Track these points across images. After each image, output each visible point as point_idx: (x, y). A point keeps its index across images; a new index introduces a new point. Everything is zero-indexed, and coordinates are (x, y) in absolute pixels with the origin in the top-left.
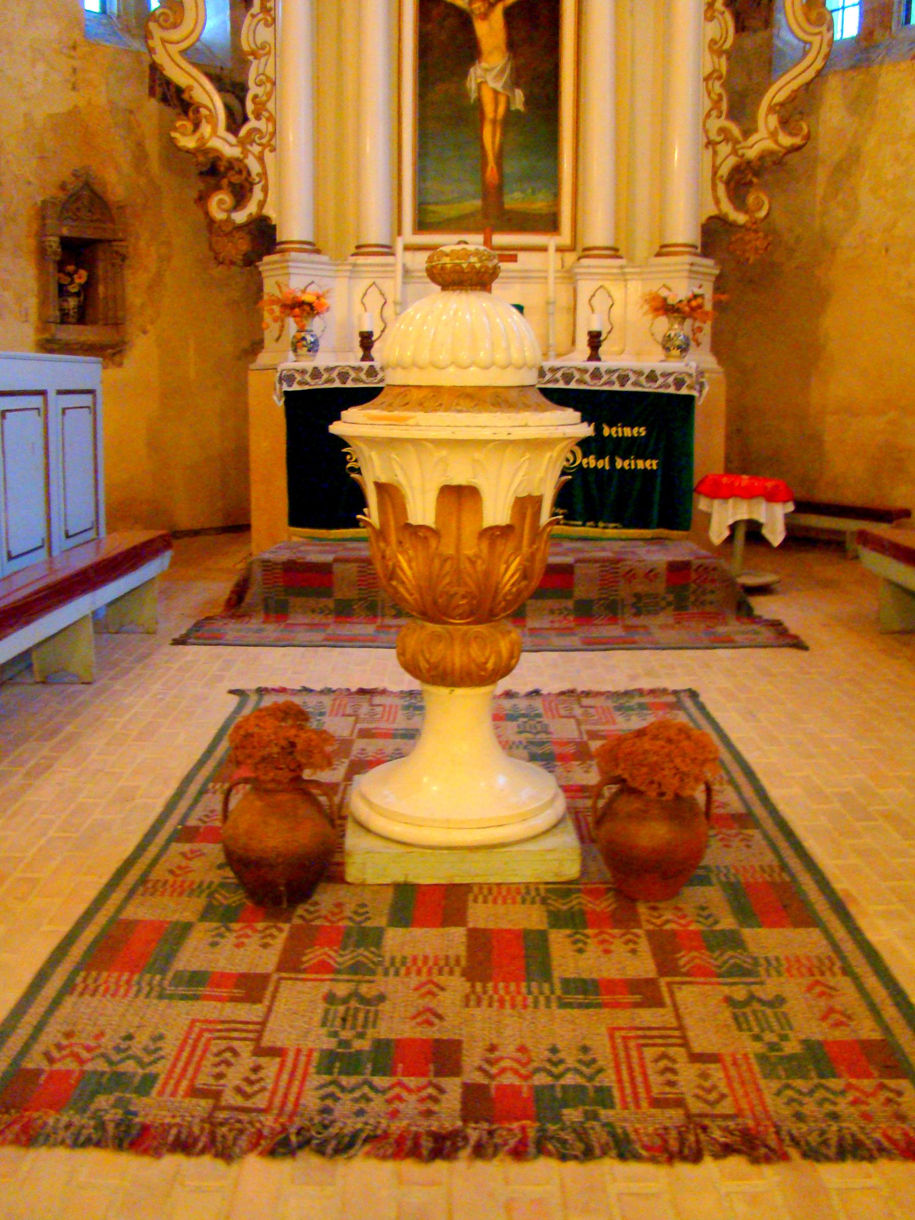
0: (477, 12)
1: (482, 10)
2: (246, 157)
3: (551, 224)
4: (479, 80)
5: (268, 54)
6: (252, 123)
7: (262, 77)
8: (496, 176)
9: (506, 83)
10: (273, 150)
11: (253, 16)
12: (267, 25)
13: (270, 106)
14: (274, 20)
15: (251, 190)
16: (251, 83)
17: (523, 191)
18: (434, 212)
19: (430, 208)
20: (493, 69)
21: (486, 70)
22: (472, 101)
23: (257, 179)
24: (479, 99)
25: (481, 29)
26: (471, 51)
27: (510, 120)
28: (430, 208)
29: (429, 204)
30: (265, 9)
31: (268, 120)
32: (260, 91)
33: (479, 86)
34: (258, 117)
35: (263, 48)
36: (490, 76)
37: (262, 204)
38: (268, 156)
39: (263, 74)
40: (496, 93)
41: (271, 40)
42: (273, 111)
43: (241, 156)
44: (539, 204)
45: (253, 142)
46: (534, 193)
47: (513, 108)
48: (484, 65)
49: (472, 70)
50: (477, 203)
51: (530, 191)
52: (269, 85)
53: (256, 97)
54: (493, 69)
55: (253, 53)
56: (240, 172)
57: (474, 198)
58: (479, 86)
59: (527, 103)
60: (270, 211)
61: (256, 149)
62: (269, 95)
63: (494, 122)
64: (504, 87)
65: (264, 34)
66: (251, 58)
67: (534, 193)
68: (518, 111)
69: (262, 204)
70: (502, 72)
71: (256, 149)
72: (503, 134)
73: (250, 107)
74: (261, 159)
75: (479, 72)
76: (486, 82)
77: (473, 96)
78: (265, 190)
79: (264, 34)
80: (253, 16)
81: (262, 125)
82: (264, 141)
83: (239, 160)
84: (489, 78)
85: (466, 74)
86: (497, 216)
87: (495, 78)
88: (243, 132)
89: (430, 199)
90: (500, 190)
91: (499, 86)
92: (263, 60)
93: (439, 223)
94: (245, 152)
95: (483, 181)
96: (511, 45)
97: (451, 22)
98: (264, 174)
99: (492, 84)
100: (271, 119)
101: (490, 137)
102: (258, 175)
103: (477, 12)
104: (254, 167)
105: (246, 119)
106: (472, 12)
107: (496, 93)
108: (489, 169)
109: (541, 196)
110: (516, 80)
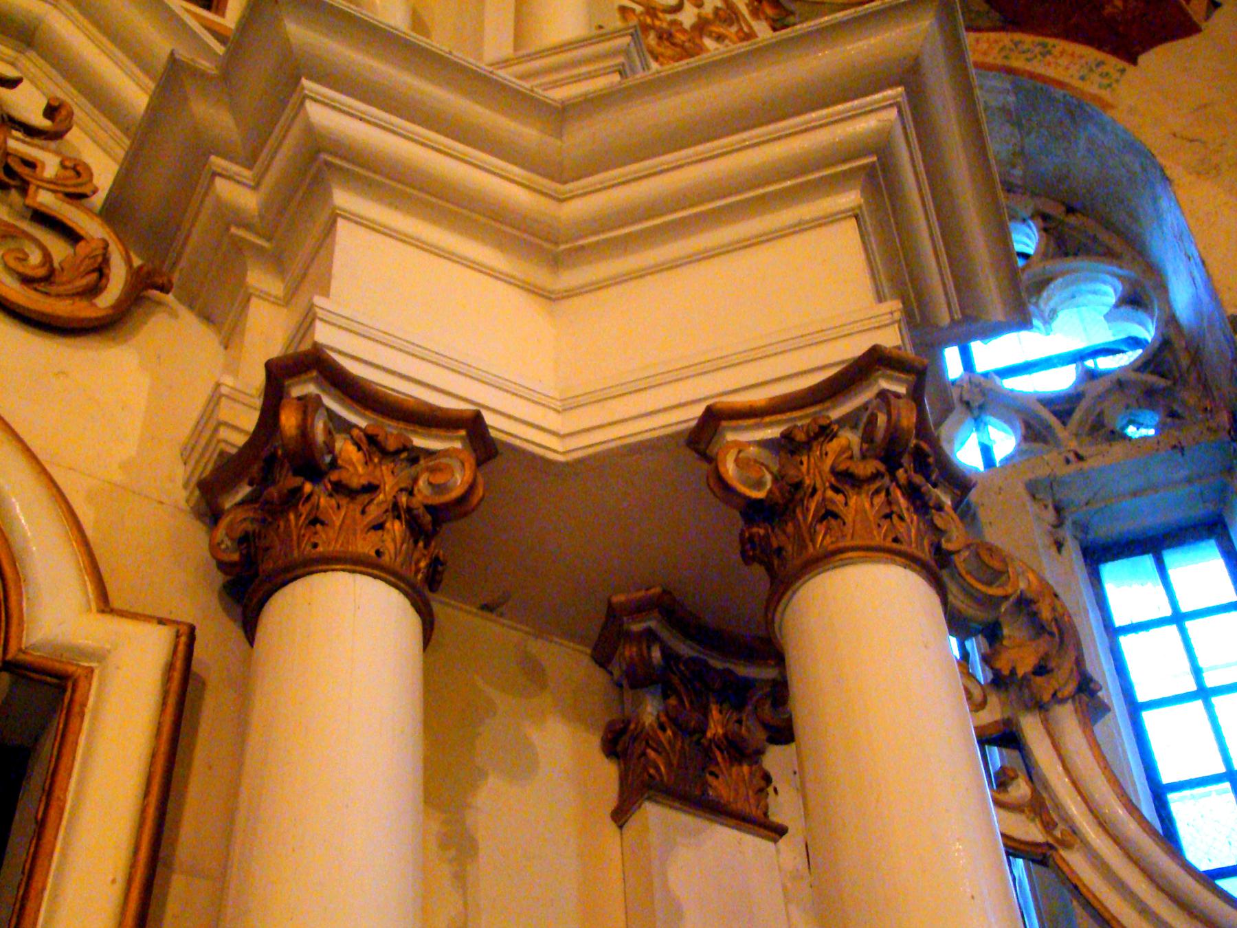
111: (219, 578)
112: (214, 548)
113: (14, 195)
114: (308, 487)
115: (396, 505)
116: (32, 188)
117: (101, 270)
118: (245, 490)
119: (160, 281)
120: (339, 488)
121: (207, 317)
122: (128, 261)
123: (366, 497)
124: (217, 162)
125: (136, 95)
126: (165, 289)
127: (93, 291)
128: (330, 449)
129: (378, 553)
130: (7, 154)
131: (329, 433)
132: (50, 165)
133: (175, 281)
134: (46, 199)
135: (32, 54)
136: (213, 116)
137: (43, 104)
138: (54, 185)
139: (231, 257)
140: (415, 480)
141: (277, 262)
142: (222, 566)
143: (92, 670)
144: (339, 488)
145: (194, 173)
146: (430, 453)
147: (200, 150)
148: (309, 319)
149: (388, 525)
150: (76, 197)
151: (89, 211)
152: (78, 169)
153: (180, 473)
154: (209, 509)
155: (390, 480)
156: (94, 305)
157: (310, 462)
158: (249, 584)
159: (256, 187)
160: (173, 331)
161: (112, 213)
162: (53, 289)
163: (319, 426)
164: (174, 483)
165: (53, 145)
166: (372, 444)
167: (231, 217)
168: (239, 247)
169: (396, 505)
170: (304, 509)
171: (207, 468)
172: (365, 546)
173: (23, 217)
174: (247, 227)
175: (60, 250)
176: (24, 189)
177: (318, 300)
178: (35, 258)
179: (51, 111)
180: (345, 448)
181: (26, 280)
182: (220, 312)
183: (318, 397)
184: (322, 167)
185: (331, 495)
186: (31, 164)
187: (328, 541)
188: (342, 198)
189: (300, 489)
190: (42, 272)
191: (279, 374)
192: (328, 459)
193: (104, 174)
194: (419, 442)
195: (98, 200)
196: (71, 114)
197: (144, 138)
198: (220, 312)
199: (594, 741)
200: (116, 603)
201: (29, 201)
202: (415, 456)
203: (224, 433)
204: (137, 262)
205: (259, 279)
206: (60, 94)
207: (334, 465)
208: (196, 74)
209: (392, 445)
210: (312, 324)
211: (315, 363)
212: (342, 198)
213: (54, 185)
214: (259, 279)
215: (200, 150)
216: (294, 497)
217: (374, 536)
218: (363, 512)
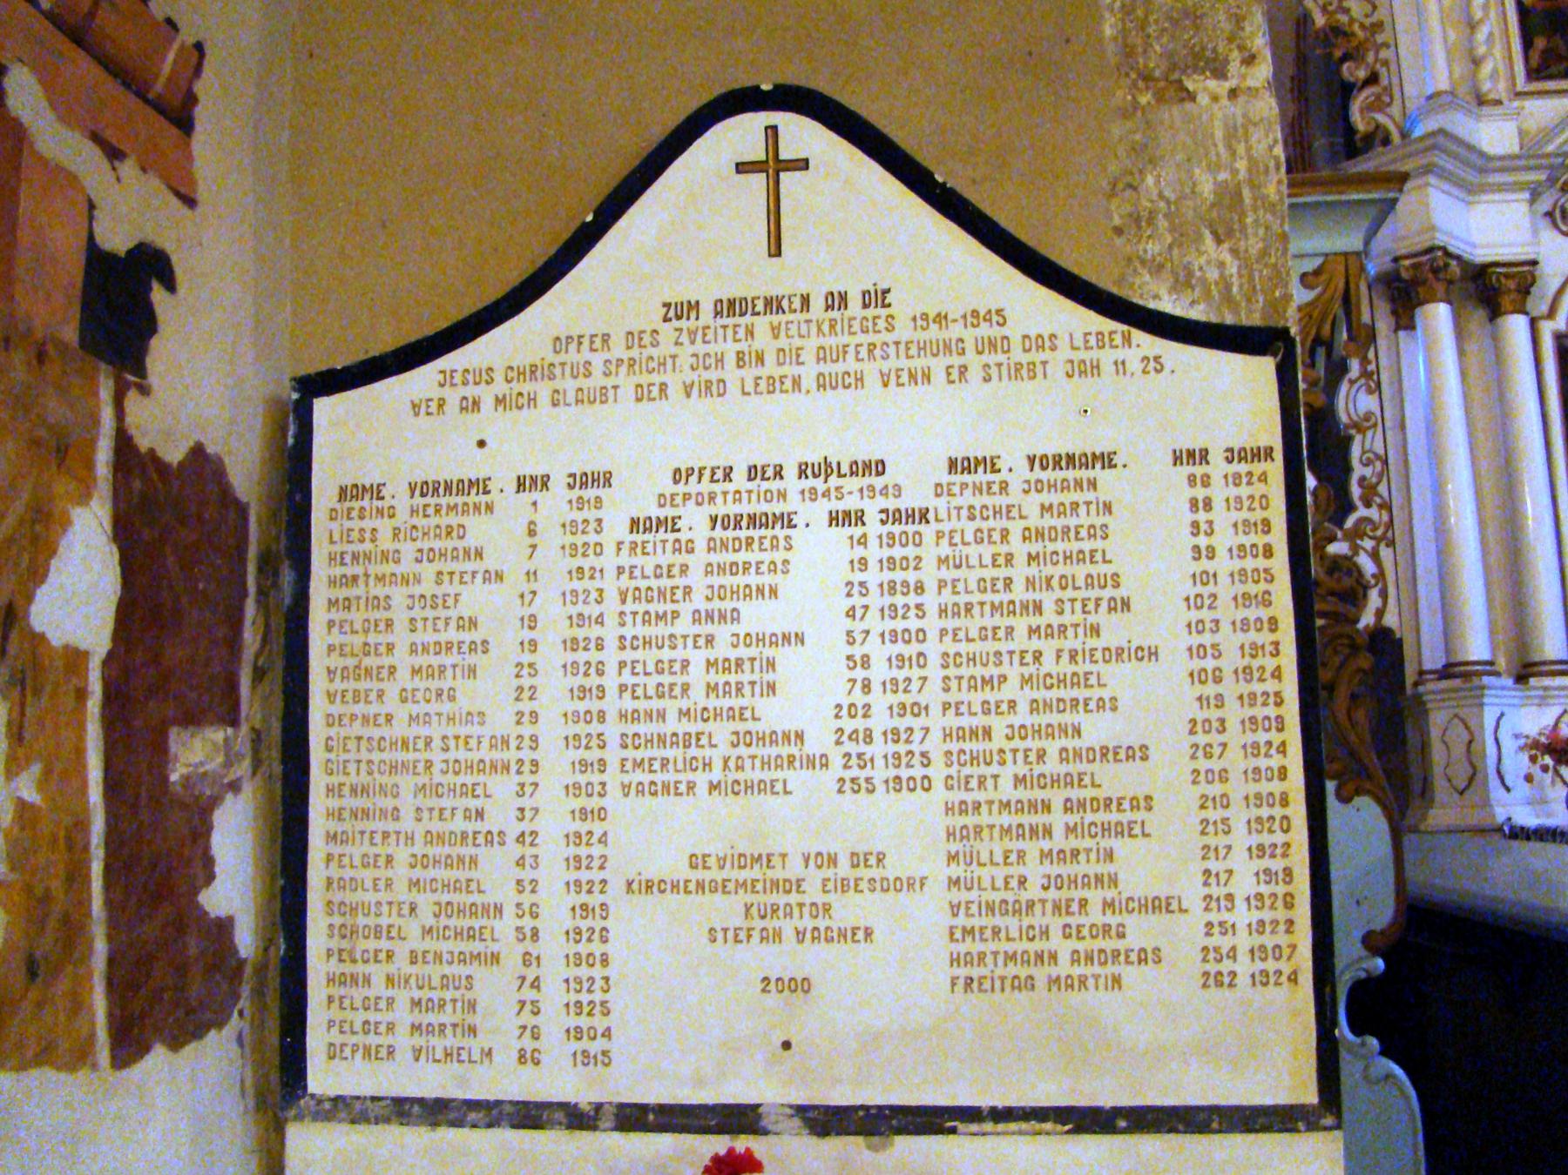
2: (1356, 553)
5: (1375, 425)
6: (1362, 512)
7: (1370, 455)
10: (1391, 543)
11: (1352, 382)
12: (1370, 392)
13: (1382, 489)
14: (1379, 384)
15: (1365, 596)
16: (1355, 462)
23: (1373, 582)
30: (1365, 374)
31: (1381, 507)
32: (1368, 472)
34: (1368, 505)
35: (1367, 419)
37: (1380, 613)
38: (1385, 553)
39: (1370, 451)
41: (1376, 409)
42: (1385, 494)
43: (1350, 553)
45: (1362, 535)
52: (1378, 465)
53: (1362, 479)
55: (1355, 425)
56: (1349, 573)
60: (1390, 620)
61: (1368, 544)
62: (1380, 476)
65: (1367, 402)
66: (1353, 432)
69: (1380, 613)
71: (1368, 544)
73: (1355, 491)
74: (1375, 555)
78: (1384, 594)
79: (1367, 402)
80: (1352, 382)
81: (1373, 513)
82: (1379, 533)
83: (1346, 557)
88: (1349, 523)
92: (1369, 434)
94: (1356, 549)
98: (1380, 575)
100: (1386, 506)
102: (1374, 576)
104: (1366, 564)
105: (1350, 508)
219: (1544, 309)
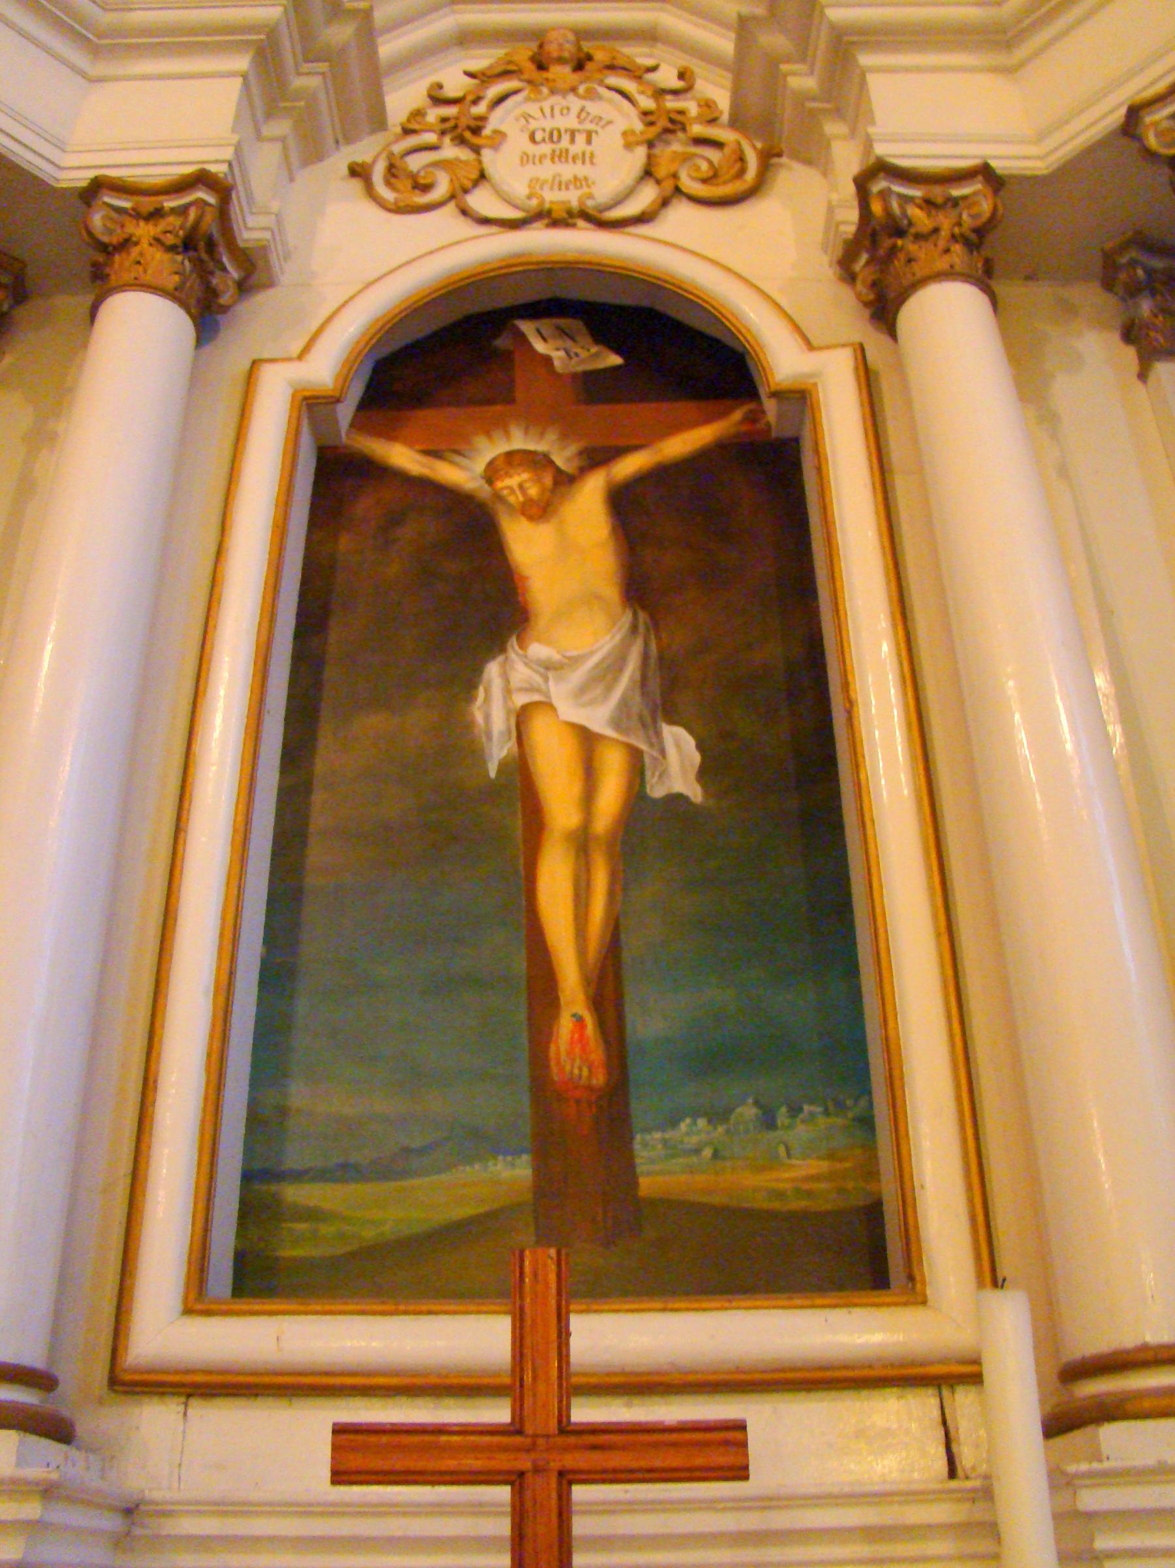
0: (516, 499)
1: (533, 491)
3: (862, 1251)
4: (520, 700)
8: (597, 1053)
9: (624, 703)
17: (718, 1115)
18: (313, 1215)
19: (293, 1194)
20: (575, 661)
21: (548, 667)
22: (493, 774)
24: (521, 771)
25: (528, 545)
26: (492, 609)
27: (648, 825)
28: (293, 1194)
29: (298, 1176)
33: (522, 719)
36: (569, 688)
40: (587, 740)
44: (793, 1166)
46: (768, 1121)
47: (657, 790)
48: (538, 650)
49: (493, 670)
50: (515, 1173)
51: (748, 1112)
54: (574, 661)
57: (497, 1149)
58: (522, 719)
59: (703, 774)
63: (582, 842)
64: (616, 724)
67: (768, 1121)
68: (676, 800)
70: (615, 665)
72: (619, 885)
75: (521, 673)
76: (548, 706)
77: (498, 751)
84: (560, 693)
85: (470, 682)
86: (604, 1223)
87: (582, 690)
89: (295, 1157)
90: (612, 1110)
91: (598, 719)
93: (334, 1263)
95: (541, 1084)
96: (638, 589)
97: (418, 529)
99: (569, 711)
101: (565, 901)
103: (516, 499)
106: (498, 497)
107: (587, 740)
108: (565, 1026)
109: (801, 1133)
110: (666, 692)
111: (867, 313)
112: (858, 296)
113: (680, 135)
114: (899, 242)
115: (953, 236)
116: (688, 128)
117: (742, 159)
118: (864, 258)
119: (775, 151)
120: (919, 237)
121: (808, 162)
122: (754, 147)
123: (934, 236)
124: (784, 68)
125: (725, 45)
126: (779, 155)
127: (742, 172)
128: (905, 215)
129: (952, 266)
130: (669, 112)
131: (902, 207)
132: (692, 107)
133: (783, 146)
134: (697, 129)
135: (659, 45)
136: (774, 41)
137: (675, 73)
138: (699, 119)
139: (809, 120)
140: (960, 216)
141: (838, 113)
142: (866, 304)
143: (815, 385)
144: (919, 237)
145: (773, 79)
146: (965, 198)
147: (773, 64)
148: (868, 143)
149: (952, 249)
150: (713, 121)
151: (722, 126)
152: (708, 105)
153: (825, 259)
154: (849, 277)
155: (945, 222)
156: (745, 181)
157: (898, 230)
158: (884, 310)
159: (812, 73)
160: (792, 177)
161: (735, 123)
162: (720, 180)
163: (895, 205)
164: (824, 267)
165: (689, 95)
166: (929, 204)
167: (803, 98)
168: (813, 114)
169: (953, 236)
170: (902, 256)
171: (839, 252)
172: (942, 264)
173: (688, 145)
174: (814, 99)
175: (714, 155)
176: (684, 129)
177: (871, 130)
178: (704, 166)
179: (681, 76)
180: (915, 212)
181: (704, 181)
182: (814, 155)
183: (889, 189)
184: (845, 47)
185: (913, 242)
186: (681, 112)
187: (919, 270)
188: (865, 59)
189: (894, 246)
190: (711, 174)
191: (862, 183)
192: (905, 222)
193: (723, 101)
194: (956, 192)
195: (725, 118)
196: (692, 73)
197: (738, 69)
198: (814, 155)
199: (1115, 338)
200: (815, 343)
201: (689, 135)
202: (955, 202)
203: (842, 228)
204: (759, 145)
205: (833, 128)
206: (685, 64)
207: (910, 224)
208: (755, 18)
209: (940, 201)
210: (871, 147)
211: (883, 168)
212: (865, 59)
213: (699, 119)
214: (833, 128)
215: (773, 64)
216: (893, 251)
217: (947, 258)
218: (935, 245)
219: (296, 348)
